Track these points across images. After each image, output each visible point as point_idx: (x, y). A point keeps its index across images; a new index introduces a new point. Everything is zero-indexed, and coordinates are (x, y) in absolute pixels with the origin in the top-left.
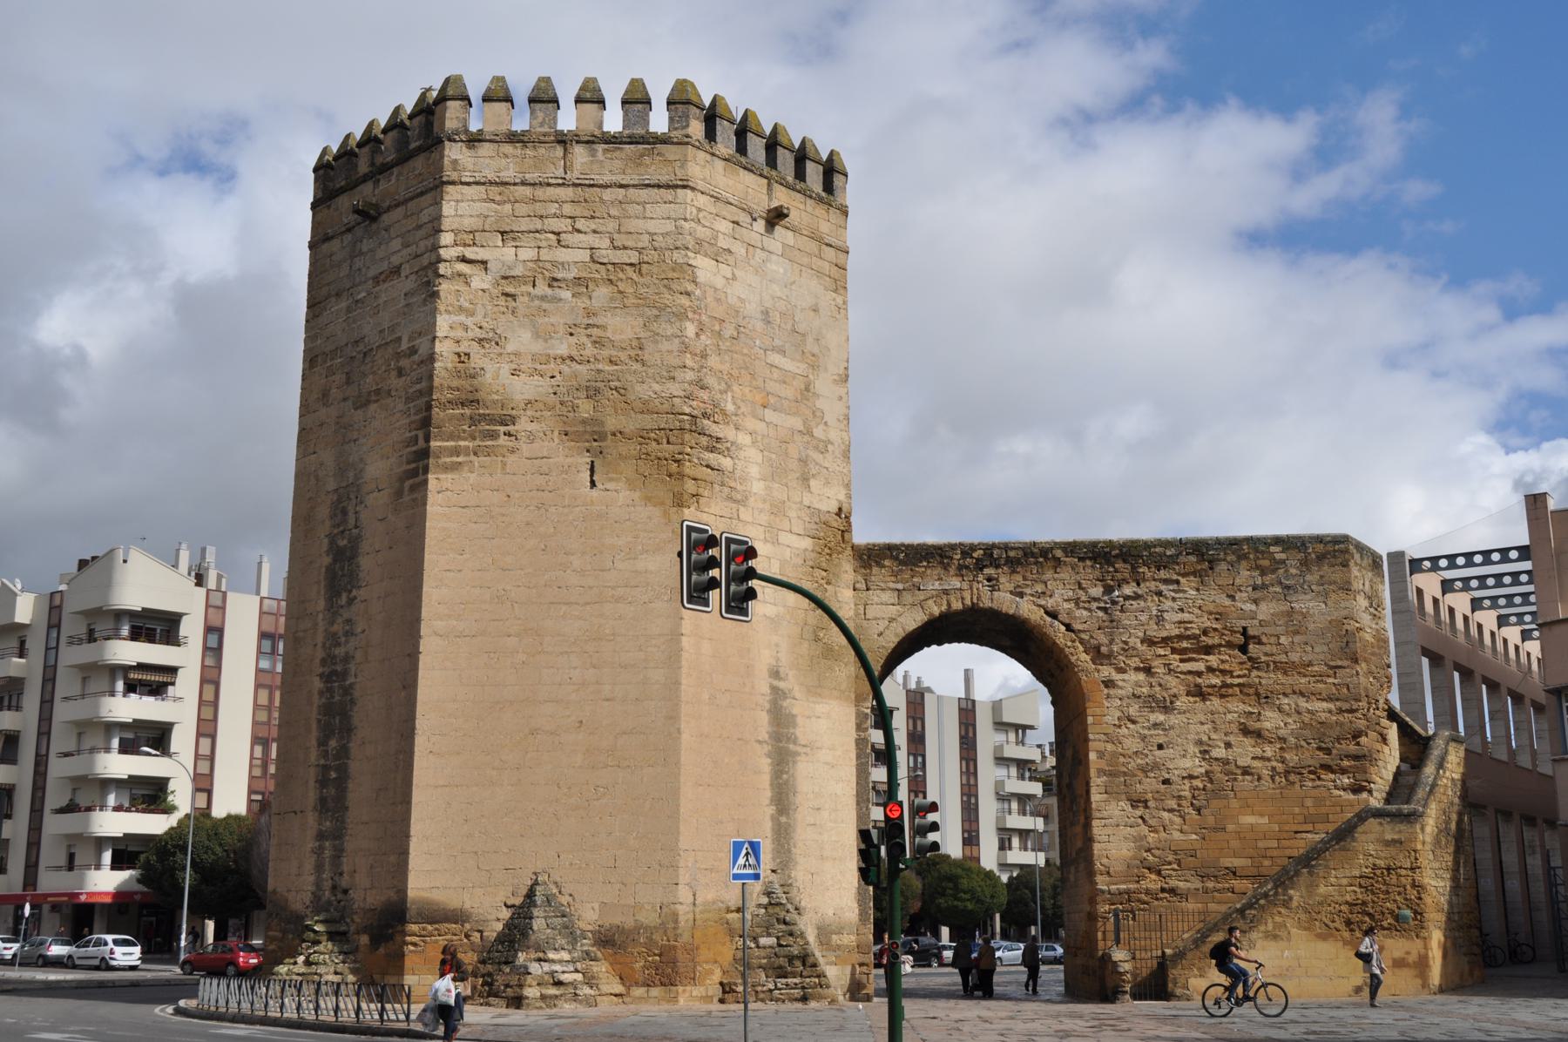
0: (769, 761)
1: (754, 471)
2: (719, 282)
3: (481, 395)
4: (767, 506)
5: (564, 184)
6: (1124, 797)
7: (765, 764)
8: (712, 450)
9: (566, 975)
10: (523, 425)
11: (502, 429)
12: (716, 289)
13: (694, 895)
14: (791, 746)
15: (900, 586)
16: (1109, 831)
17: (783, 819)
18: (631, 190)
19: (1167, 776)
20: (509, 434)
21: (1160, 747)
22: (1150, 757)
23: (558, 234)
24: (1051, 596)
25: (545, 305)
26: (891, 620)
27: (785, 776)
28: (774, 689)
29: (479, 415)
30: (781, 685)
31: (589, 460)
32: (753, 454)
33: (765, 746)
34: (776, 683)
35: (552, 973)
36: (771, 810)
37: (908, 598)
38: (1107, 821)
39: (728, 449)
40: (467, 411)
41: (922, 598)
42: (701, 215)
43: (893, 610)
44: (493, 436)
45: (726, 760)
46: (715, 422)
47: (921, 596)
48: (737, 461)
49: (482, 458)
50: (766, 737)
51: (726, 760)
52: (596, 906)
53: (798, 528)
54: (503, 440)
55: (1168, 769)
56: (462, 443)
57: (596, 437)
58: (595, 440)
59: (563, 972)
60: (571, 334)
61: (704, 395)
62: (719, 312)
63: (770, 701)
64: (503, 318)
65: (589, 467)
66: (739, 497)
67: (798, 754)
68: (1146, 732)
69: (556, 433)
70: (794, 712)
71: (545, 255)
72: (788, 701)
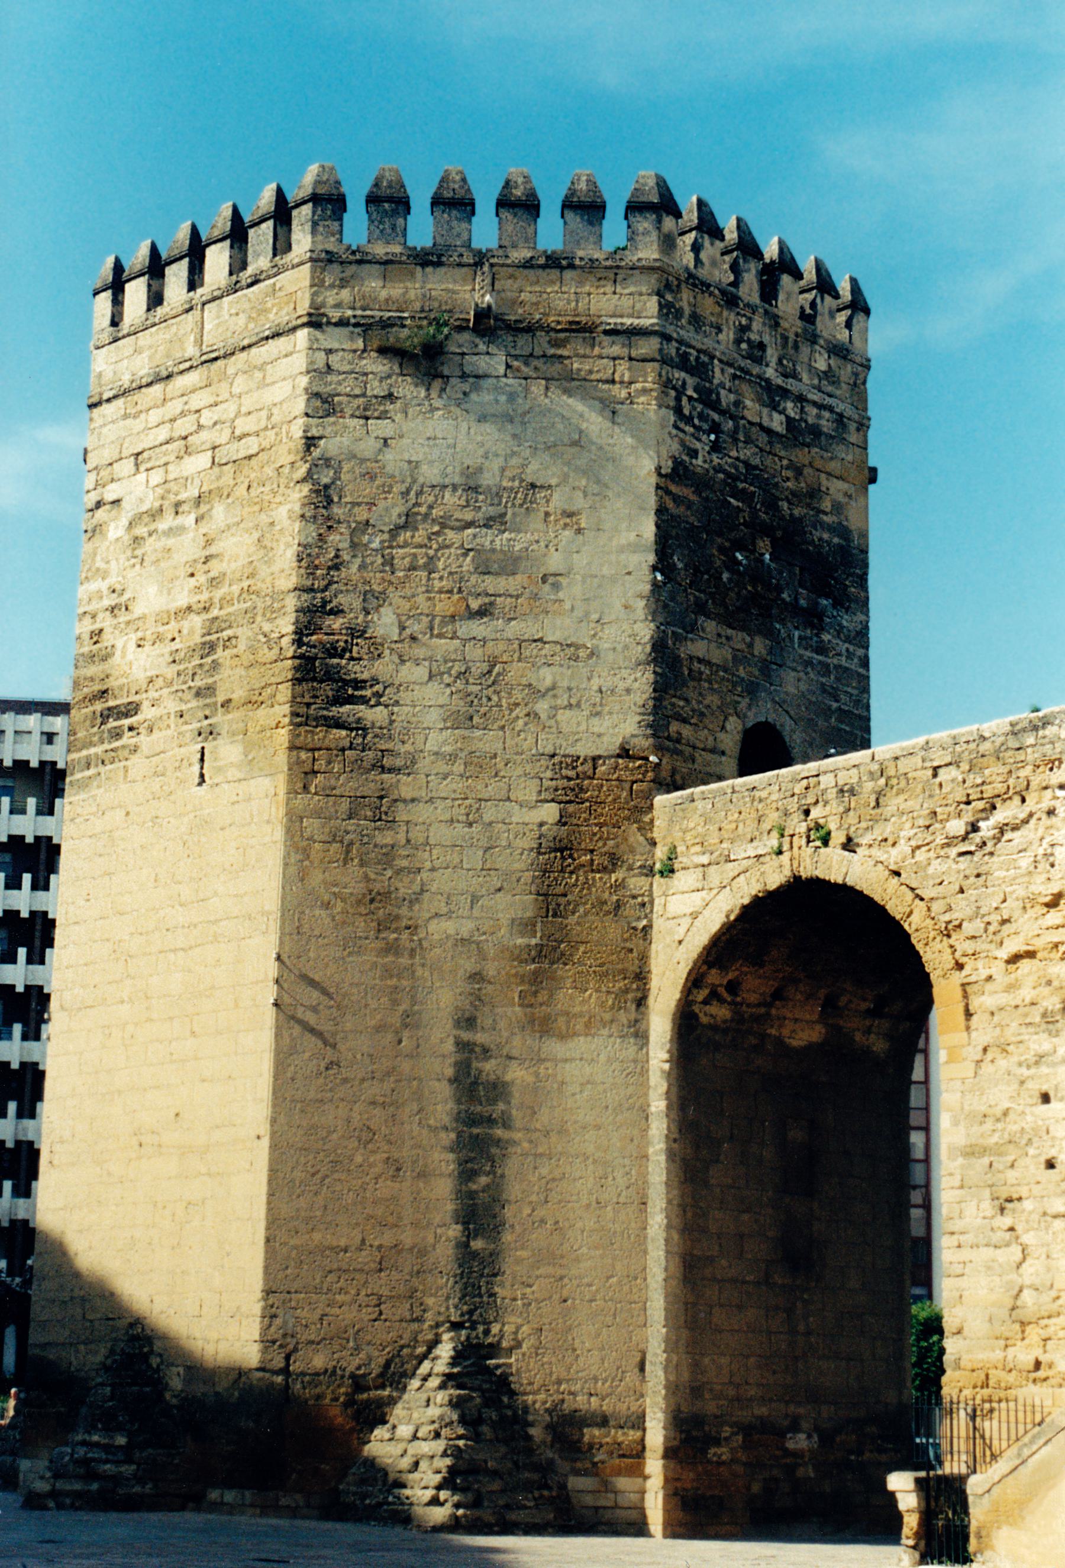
0: (451, 1156)
1: (433, 717)
2: (368, 447)
3: (112, 683)
4: (459, 768)
5: (191, 367)
6: (987, 1193)
7: (445, 1162)
8: (351, 700)
9: (108, 1466)
10: (147, 713)
11: (126, 722)
12: (363, 461)
13: (287, 1358)
14: (499, 1132)
15: (705, 859)
16: (966, 1254)
17: (477, 1244)
18: (254, 350)
19: (1052, 1153)
20: (131, 729)
21: (1046, 1098)
22: (1029, 1118)
23: (185, 438)
24: (894, 844)
25: (171, 542)
26: (695, 915)
27: (483, 1180)
28: (463, 1046)
29: (109, 709)
30: (480, 1038)
31: (199, 747)
32: (435, 694)
33: (443, 1135)
34: (466, 1036)
35: (85, 1462)
36: (455, 1231)
37: (715, 875)
38: (962, 1238)
39: (378, 695)
40: (99, 706)
41: (732, 874)
42: (334, 359)
43: (697, 900)
44: (117, 734)
45: (359, 1159)
46: (352, 659)
47: (731, 869)
48: (396, 709)
49: (109, 767)
50: (446, 1120)
51: (359, 1159)
52: (181, 1370)
53: (528, 791)
54: (127, 739)
55: (1053, 1138)
56: (93, 751)
57: (207, 713)
58: (206, 717)
59: (107, 1461)
60: (192, 575)
61: (337, 623)
62: (368, 490)
63: (456, 1064)
64: (130, 574)
65: (199, 756)
66: (399, 762)
67: (515, 1143)
68: (1024, 1071)
69: (172, 716)
70: (508, 1078)
71: (174, 471)
72: (493, 1061)
